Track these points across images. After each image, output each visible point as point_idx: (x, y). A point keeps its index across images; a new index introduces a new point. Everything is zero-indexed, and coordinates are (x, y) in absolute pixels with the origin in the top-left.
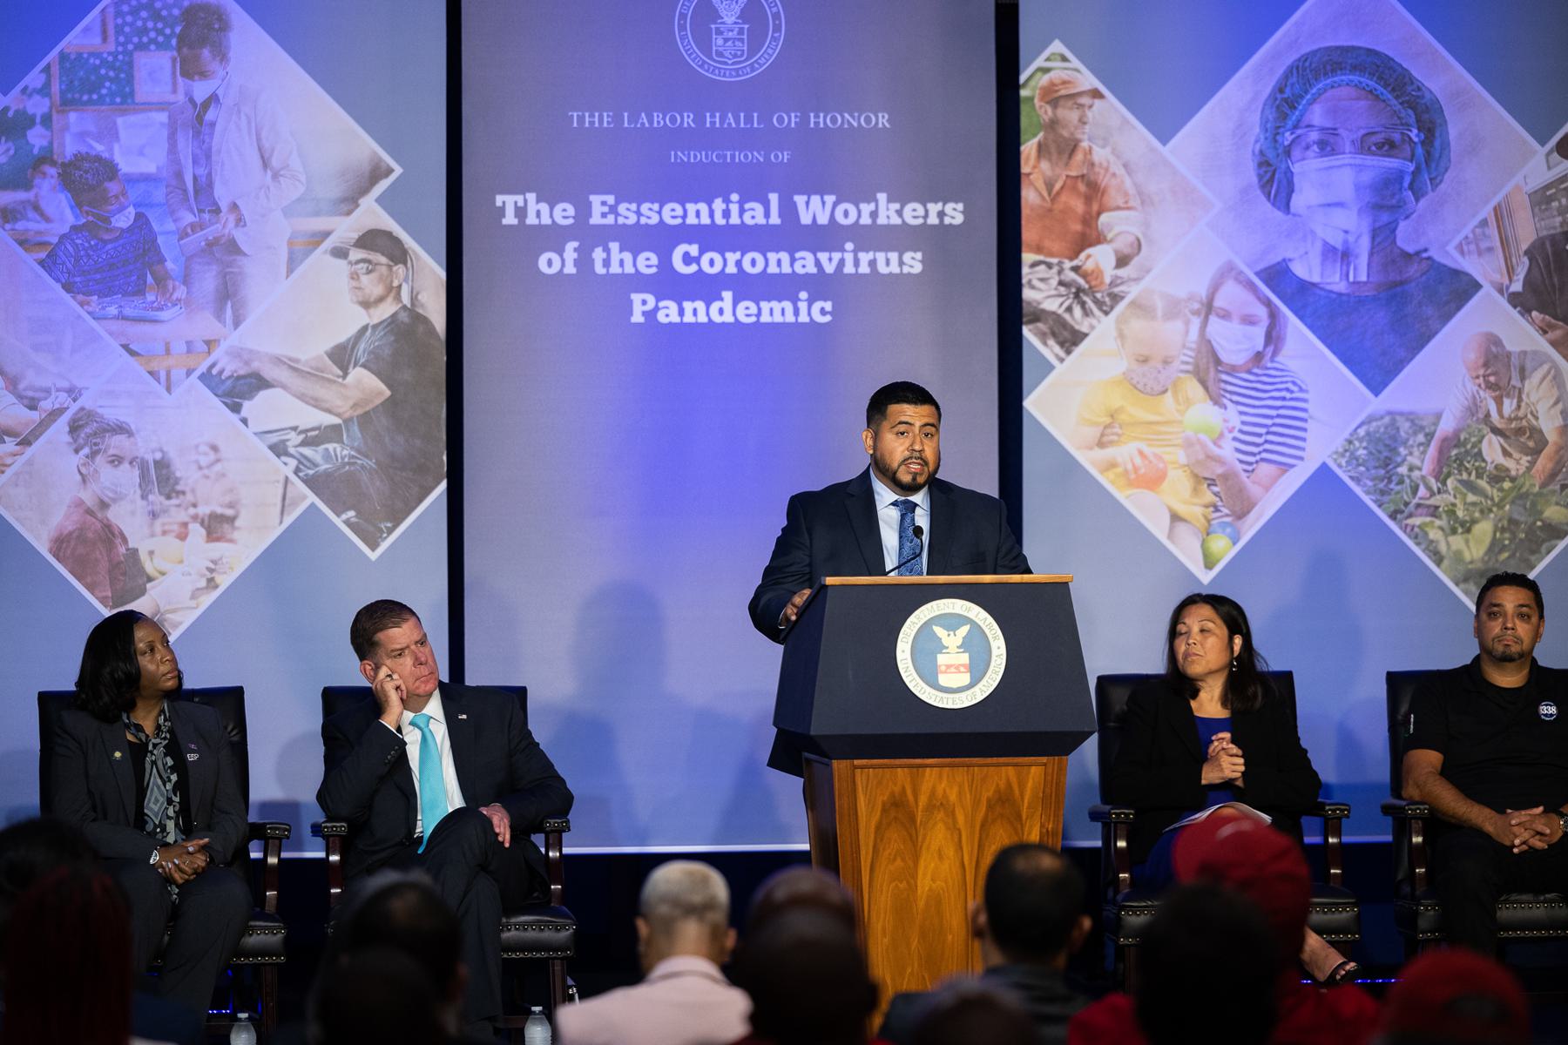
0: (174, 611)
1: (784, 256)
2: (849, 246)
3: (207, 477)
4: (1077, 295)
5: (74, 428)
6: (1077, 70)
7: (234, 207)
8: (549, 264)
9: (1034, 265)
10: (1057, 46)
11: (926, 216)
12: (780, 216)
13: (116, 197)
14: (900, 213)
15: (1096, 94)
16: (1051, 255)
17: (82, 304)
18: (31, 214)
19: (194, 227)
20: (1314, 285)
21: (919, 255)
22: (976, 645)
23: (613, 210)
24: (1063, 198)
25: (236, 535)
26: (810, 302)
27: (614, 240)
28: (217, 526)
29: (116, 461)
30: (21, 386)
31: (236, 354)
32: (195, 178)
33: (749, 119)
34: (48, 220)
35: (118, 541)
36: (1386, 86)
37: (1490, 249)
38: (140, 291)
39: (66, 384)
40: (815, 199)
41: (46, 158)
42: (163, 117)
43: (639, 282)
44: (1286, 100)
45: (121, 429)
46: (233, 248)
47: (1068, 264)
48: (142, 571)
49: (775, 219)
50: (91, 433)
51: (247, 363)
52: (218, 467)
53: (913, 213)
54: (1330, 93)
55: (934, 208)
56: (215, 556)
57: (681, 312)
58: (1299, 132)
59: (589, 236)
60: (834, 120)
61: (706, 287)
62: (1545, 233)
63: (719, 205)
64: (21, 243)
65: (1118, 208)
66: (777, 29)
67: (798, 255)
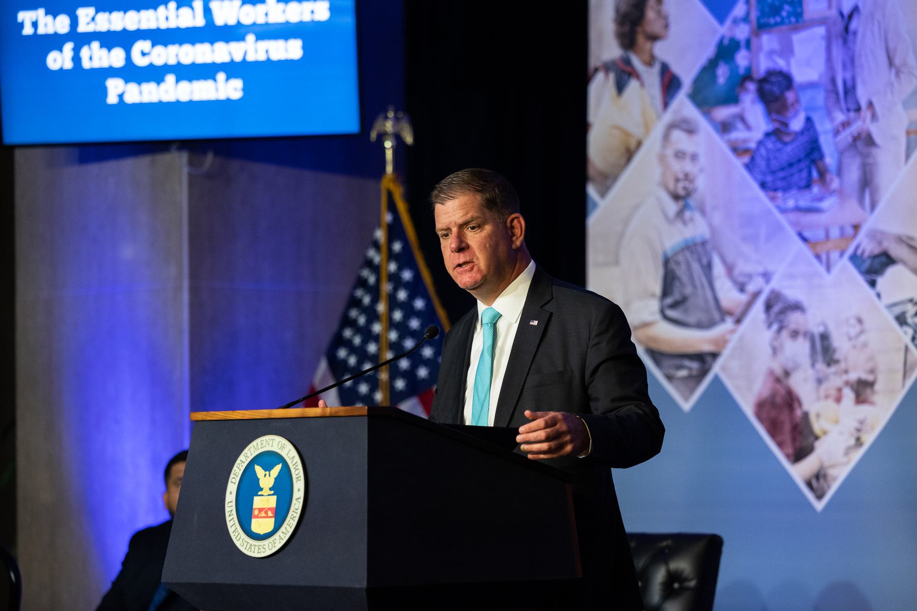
0: (833, 466)
3: (854, 347)
5: (768, 307)
7: (870, 105)
13: (793, 105)
17: (773, 199)
18: (740, 125)
19: (846, 125)
22: (283, 488)
25: (877, 398)
28: (862, 390)
29: (795, 334)
30: (737, 272)
31: (874, 235)
32: (845, 83)
34: (748, 127)
35: (796, 405)
38: (808, 186)
39: (760, 269)
41: (748, 77)
42: (821, 31)
45: (797, 307)
46: (870, 141)
48: (811, 431)
50: (779, 309)
51: (880, 243)
52: (862, 338)
56: (861, 416)
64: (737, 150)
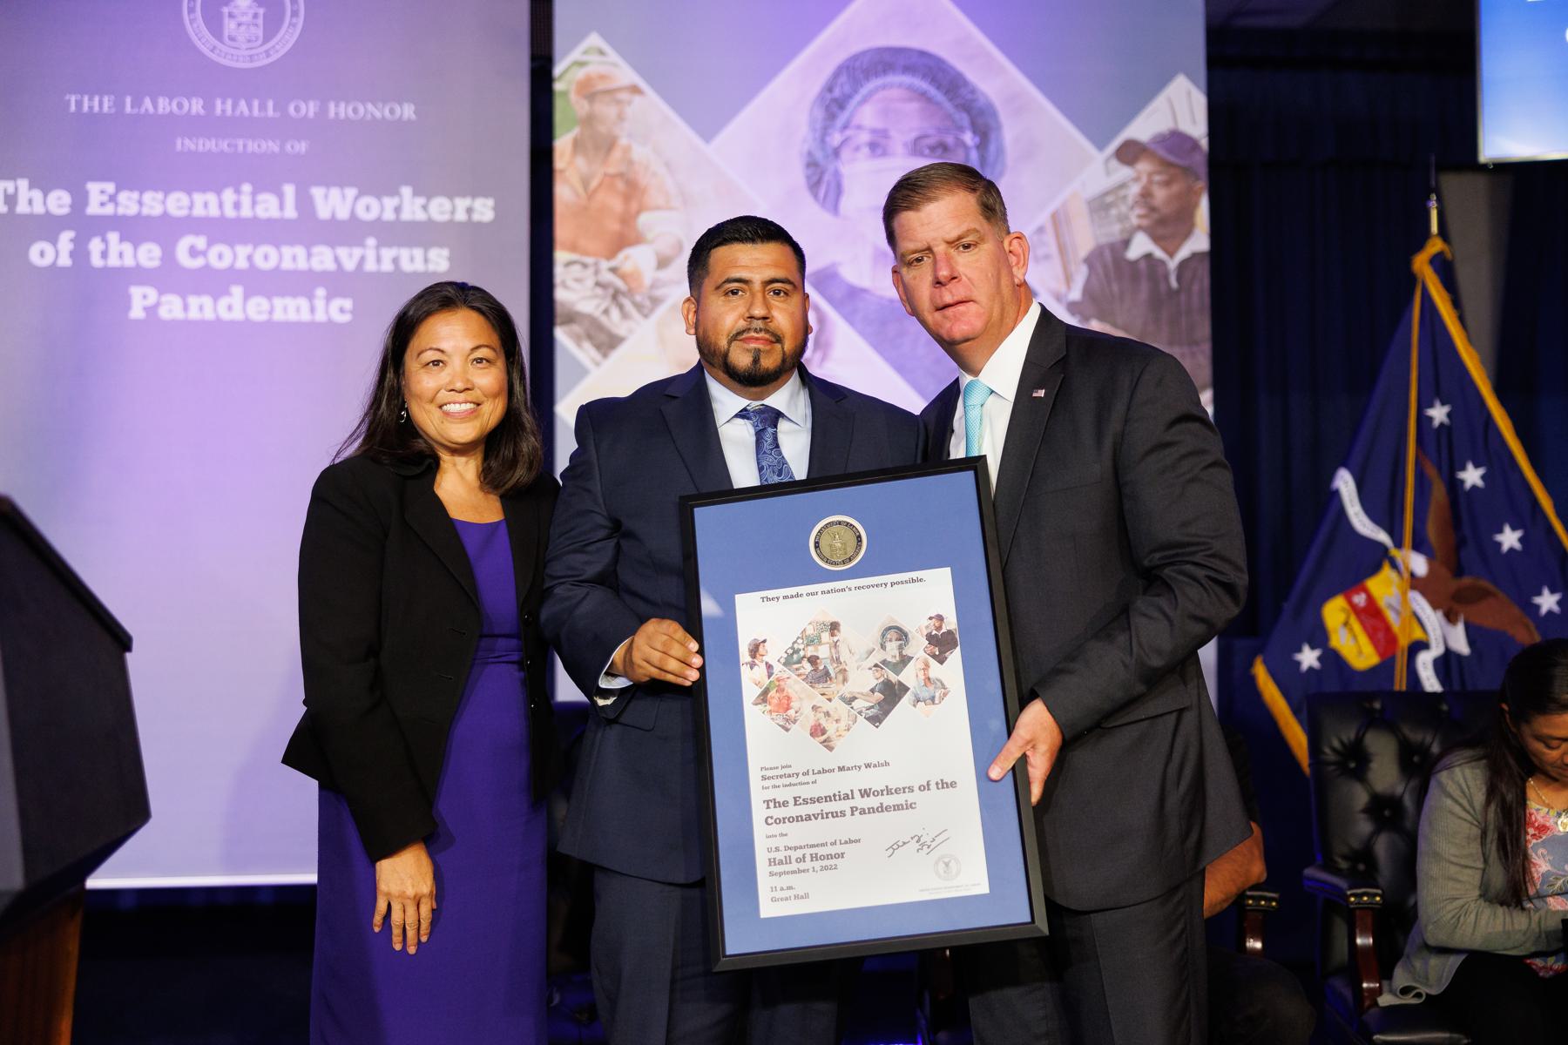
1: (300, 251)
2: (371, 242)
4: (615, 297)
6: (615, 65)
8: (41, 254)
9: (568, 264)
10: (594, 40)
11: (453, 212)
12: (298, 207)
14: (425, 208)
15: (635, 90)
16: (586, 253)
20: (864, 291)
21: (445, 252)
23: (113, 199)
24: (600, 197)
26: (328, 299)
27: (114, 229)
33: (263, 107)
36: (938, 88)
37: (1047, 257)
40: (335, 192)
43: (139, 275)
44: (835, 100)
47: (605, 265)
49: (291, 212)
53: (440, 209)
54: (881, 94)
55: (462, 203)
57: (186, 308)
58: (849, 132)
59: (85, 226)
60: (355, 110)
61: (213, 282)
62: (1104, 240)
63: (229, 196)
65: (658, 208)
66: (295, 14)
67: (317, 249)
